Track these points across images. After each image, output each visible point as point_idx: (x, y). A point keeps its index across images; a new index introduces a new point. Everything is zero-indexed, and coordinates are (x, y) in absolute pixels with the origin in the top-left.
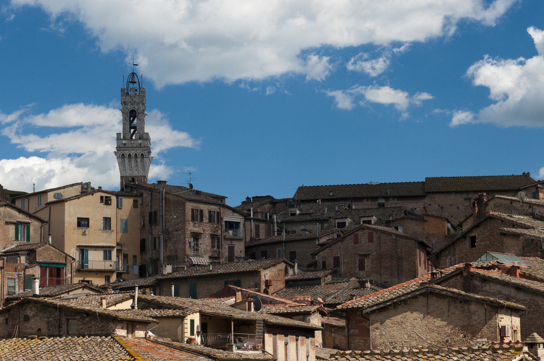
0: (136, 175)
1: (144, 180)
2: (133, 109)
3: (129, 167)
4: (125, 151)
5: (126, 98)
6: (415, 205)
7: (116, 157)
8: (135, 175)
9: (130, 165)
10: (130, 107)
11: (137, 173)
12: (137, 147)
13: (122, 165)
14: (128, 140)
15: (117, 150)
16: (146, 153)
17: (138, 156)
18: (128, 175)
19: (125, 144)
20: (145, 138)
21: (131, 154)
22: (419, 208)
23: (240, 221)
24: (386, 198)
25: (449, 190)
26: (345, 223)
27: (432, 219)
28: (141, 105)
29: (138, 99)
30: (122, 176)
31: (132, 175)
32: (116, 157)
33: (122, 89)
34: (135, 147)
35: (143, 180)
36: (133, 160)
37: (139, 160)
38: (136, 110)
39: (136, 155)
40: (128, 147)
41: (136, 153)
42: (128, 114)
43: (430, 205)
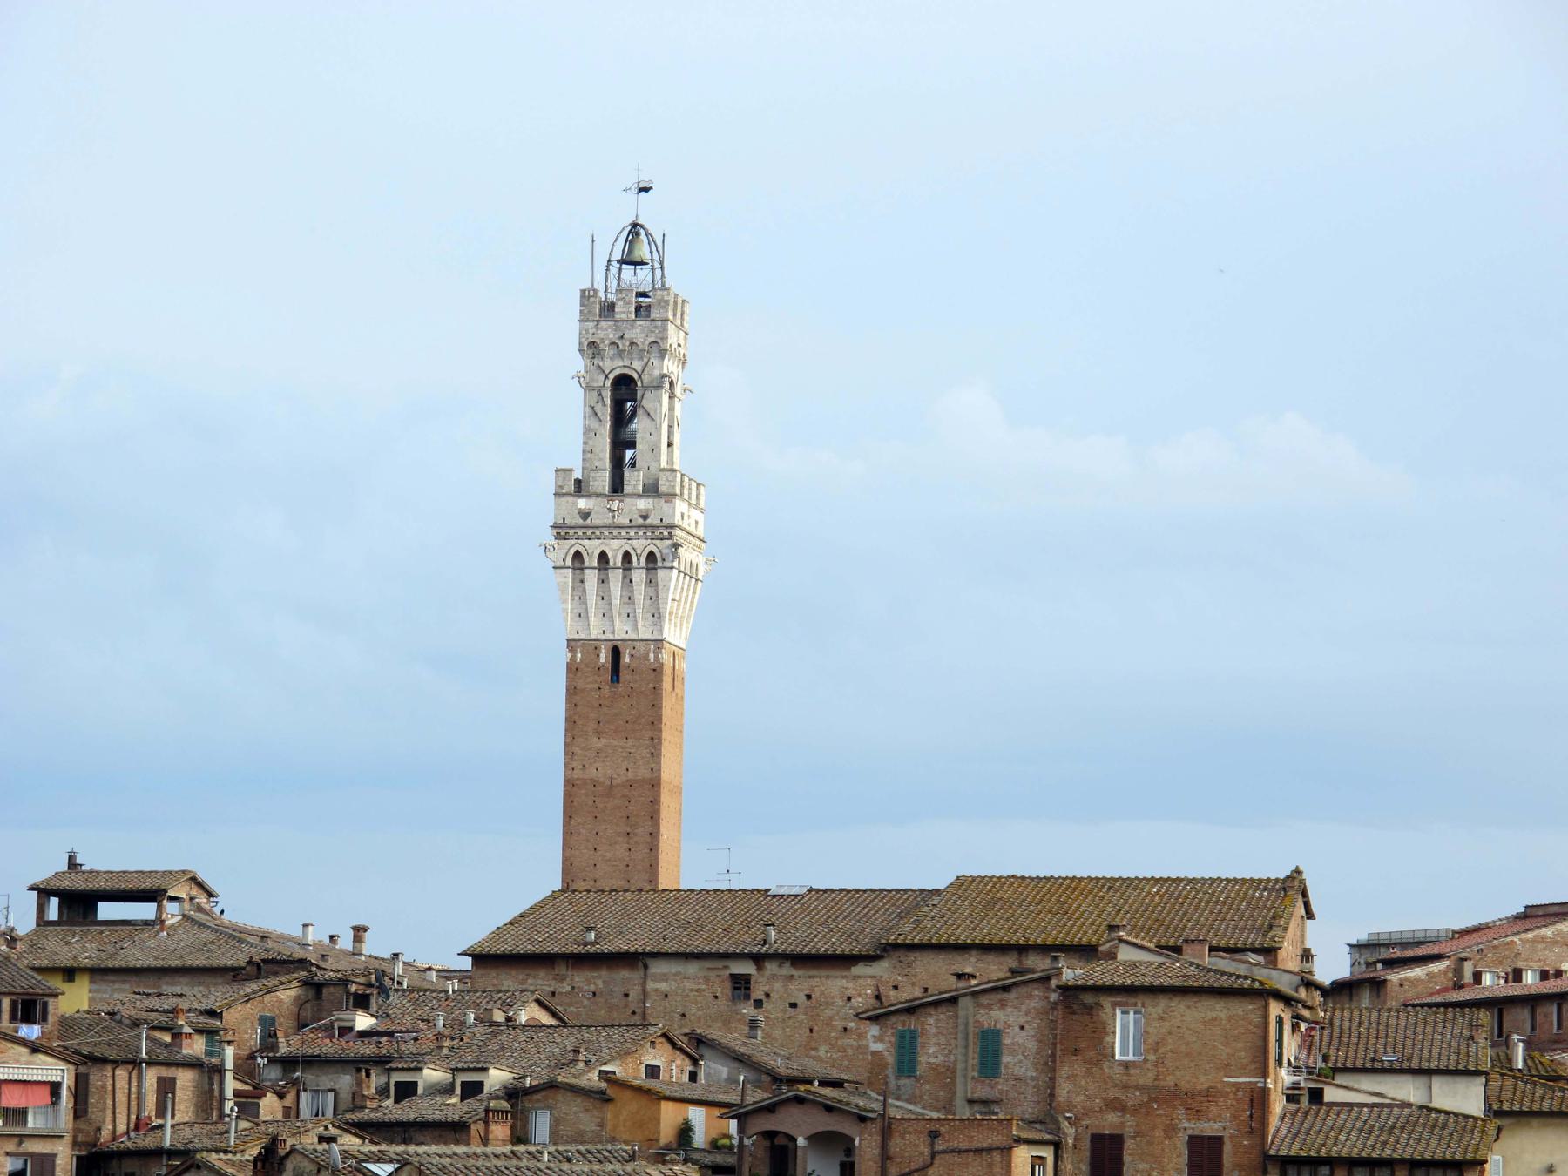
0: (627, 637)
1: (656, 657)
2: (626, 371)
3: (600, 602)
6: (850, 985)
9: (604, 597)
10: (615, 366)
14: (598, 495)
16: (665, 551)
17: (634, 559)
19: (585, 515)
21: (610, 555)
22: (860, 995)
23: (59, 1079)
24: (758, 959)
25: (964, 938)
26: (416, 1083)
27: (628, 1094)
29: (642, 331)
30: (574, 640)
31: (611, 637)
33: (583, 291)
35: (652, 655)
36: (616, 577)
37: (639, 576)
38: (635, 376)
39: (627, 557)
40: (597, 527)
42: (607, 395)
43: (896, 988)
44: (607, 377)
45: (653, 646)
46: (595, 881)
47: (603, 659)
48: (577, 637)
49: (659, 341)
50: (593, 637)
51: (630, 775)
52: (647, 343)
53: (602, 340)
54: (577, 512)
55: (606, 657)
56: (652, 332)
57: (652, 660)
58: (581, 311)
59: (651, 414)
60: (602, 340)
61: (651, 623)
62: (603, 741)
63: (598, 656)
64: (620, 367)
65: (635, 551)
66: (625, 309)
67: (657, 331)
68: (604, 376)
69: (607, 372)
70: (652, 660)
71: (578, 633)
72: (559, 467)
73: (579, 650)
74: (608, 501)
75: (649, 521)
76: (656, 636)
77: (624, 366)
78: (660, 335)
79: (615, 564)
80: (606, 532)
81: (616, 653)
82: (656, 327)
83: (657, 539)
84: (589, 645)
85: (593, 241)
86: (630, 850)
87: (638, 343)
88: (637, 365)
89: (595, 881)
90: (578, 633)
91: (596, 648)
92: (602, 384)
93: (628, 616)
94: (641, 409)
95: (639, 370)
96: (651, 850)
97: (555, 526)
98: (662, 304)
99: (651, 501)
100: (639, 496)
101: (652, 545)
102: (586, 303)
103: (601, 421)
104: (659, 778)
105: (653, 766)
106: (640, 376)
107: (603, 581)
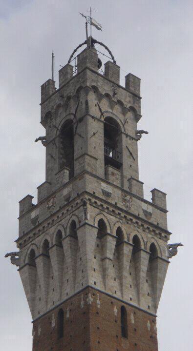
2: (68, 118)
7: (18, 268)
11: (68, 290)
12: (61, 208)
13: (31, 287)
15: (20, 246)
16: (80, 215)
17: (63, 234)
18: (50, 306)
19: (34, 221)
21: (49, 240)
31: (58, 303)
32: (18, 268)
34: (55, 214)
35: (82, 303)
36: (53, 253)
38: (72, 117)
44: (58, 129)
45: (82, 296)
47: (53, 325)
48: (38, 316)
49: (82, 85)
50: (48, 310)
52: (76, 90)
54: (30, 222)
55: (55, 321)
56: (78, 82)
57: (82, 306)
60: (53, 107)
61: (81, 278)
63: (51, 323)
65: (63, 226)
70: (82, 306)
73: (39, 326)
75: (71, 199)
76: (85, 286)
77: (66, 116)
78: (83, 80)
79: (52, 243)
81: (61, 314)
85: (53, 57)
88: (73, 111)
91: (49, 318)
95: (74, 113)
99: (71, 186)
100: (65, 185)
103: (55, 160)
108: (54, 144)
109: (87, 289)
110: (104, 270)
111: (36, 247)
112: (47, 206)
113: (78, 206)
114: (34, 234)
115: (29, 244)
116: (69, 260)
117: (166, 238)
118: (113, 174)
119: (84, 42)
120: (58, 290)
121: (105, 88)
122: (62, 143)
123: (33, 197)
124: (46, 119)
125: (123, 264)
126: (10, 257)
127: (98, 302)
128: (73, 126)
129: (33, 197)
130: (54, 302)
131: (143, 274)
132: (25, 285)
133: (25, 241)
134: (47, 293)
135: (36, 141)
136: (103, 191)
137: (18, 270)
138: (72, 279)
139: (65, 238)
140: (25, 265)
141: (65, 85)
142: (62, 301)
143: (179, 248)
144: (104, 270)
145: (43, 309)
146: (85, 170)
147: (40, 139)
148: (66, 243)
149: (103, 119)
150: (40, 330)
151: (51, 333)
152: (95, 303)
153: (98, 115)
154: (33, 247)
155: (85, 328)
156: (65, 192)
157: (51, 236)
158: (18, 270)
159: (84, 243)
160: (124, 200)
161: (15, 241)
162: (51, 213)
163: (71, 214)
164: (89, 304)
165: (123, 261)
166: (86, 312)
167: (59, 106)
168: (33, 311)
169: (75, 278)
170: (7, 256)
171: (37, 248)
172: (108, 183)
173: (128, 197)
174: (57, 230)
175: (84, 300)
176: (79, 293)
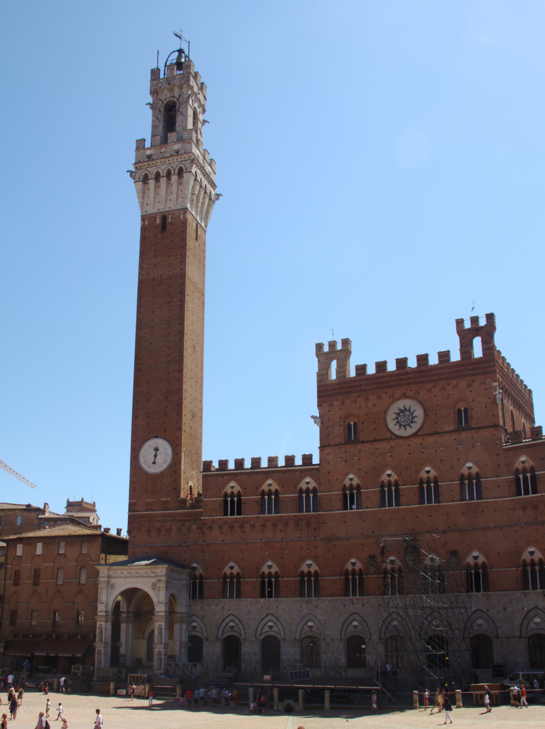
0: (170, 210)
2: (172, 98)
4: (150, 169)
5: (158, 83)
7: (134, 181)
8: (168, 209)
10: (166, 96)
11: (171, 205)
12: (171, 156)
13: (143, 194)
16: (188, 165)
17: (173, 172)
18: (155, 211)
19: (149, 157)
20: (187, 138)
21: (161, 172)
28: (184, 90)
30: (144, 215)
31: (162, 211)
32: (134, 181)
33: (152, 70)
35: (182, 216)
36: (163, 181)
38: (176, 100)
41: (169, 167)
42: (162, 109)
44: (163, 102)
45: (182, 212)
46: (152, 328)
47: (158, 222)
48: (146, 214)
50: (154, 212)
51: (171, 273)
52: (181, 84)
53: (160, 88)
54: (145, 156)
55: (160, 220)
56: (183, 79)
57: (182, 218)
58: (151, 78)
59: (183, 113)
60: (160, 88)
62: (158, 259)
63: (156, 221)
64: (169, 98)
65: (173, 167)
66: (171, 73)
67: (185, 78)
68: (161, 103)
69: (163, 101)
70: (182, 218)
71: (146, 212)
72: (137, 139)
73: (146, 220)
74: (160, 149)
75: (180, 153)
76: (184, 207)
77: (171, 97)
78: (187, 79)
79: (163, 175)
80: (158, 161)
81: (164, 218)
82: (184, 77)
83: (184, 161)
84: (151, 216)
85: (158, 53)
86: (170, 310)
87: (177, 85)
88: (177, 95)
89: (152, 328)
90: (146, 212)
91: (155, 218)
92: (160, 106)
93: (171, 200)
94: (179, 113)
95: (178, 97)
96: (181, 308)
97: (136, 163)
98: (188, 67)
99: (181, 145)
100: (175, 143)
101: (181, 164)
102: (153, 74)
104: (185, 273)
105: (181, 267)
106: (178, 99)
107: (157, 187)
108: (160, 111)
109: (185, 210)
110: (193, 200)
111: (149, 173)
112: (160, 151)
113: (185, 159)
114: (148, 165)
115: (144, 169)
116: (174, 188)
117: (214, 189)
118: (201, 145)
119: (177, 50)
120: (164, 204)
121: (196, 89)
122: (164, 112)
123: (144, 140)
124: (154, 92)
125: (199, 199)
126: (129, 173)
127: (190, 218)
128: (175, 106)
129: (144, 140)
130: (159, 210)
131: (205, 207)
132: (138, 192)
133: (140, 166)
134: (154, 203)
135: (147, 104)
136: (197, 154)
137: (134, 182)
138: (175, 200)
139: (173, 175)
140: (140, 181)
141: (172, 77)
142: (165, 210)
143: (220, 197)
144: (193, 200)
145: (151, 210)
146: (192, 139)
147: (149, 104)
148: (174, 178)
149: (193, 107)
150: (146, 223)
151: (156, 227)
152: (189, 218)
153: (191, 104)
154: (146, 172)
155: (183, 231)
156: (176, 147)
157: (163, 170)
158: (134, 182)
159: (188, 182)
160: (204, 162)
161: (133, 164)
162: (163, 156)
163: (180, 163)
164: (187, 219)
165: (200, 198)
166: (184, 223)
167: (165, 88)
168: (142, 210)
169: (177, 200)
170: (128, 171)
171: (150, 174)
172: (199, 150)
173: (205, 161)
174: (167, 169)
175: (183, 214)
176: (179, 209)
